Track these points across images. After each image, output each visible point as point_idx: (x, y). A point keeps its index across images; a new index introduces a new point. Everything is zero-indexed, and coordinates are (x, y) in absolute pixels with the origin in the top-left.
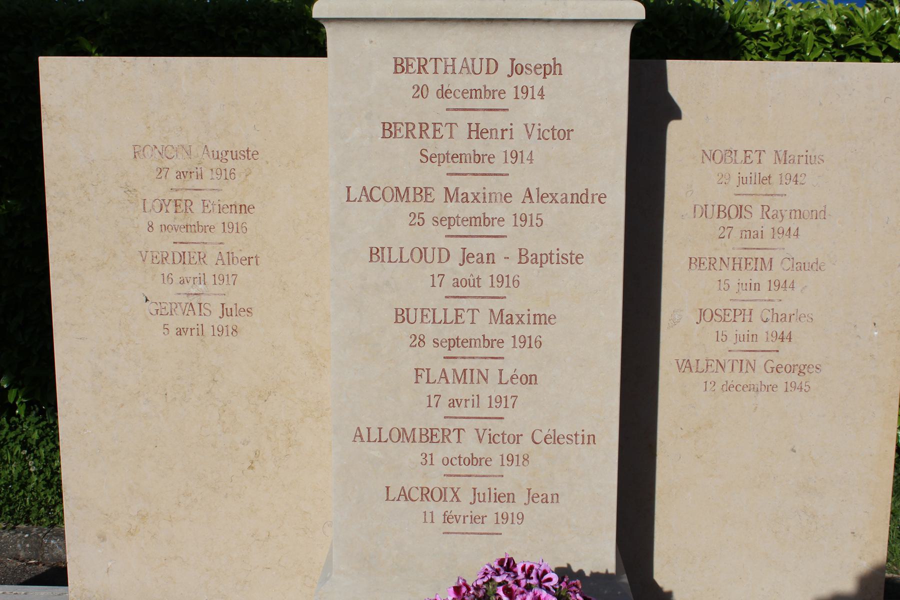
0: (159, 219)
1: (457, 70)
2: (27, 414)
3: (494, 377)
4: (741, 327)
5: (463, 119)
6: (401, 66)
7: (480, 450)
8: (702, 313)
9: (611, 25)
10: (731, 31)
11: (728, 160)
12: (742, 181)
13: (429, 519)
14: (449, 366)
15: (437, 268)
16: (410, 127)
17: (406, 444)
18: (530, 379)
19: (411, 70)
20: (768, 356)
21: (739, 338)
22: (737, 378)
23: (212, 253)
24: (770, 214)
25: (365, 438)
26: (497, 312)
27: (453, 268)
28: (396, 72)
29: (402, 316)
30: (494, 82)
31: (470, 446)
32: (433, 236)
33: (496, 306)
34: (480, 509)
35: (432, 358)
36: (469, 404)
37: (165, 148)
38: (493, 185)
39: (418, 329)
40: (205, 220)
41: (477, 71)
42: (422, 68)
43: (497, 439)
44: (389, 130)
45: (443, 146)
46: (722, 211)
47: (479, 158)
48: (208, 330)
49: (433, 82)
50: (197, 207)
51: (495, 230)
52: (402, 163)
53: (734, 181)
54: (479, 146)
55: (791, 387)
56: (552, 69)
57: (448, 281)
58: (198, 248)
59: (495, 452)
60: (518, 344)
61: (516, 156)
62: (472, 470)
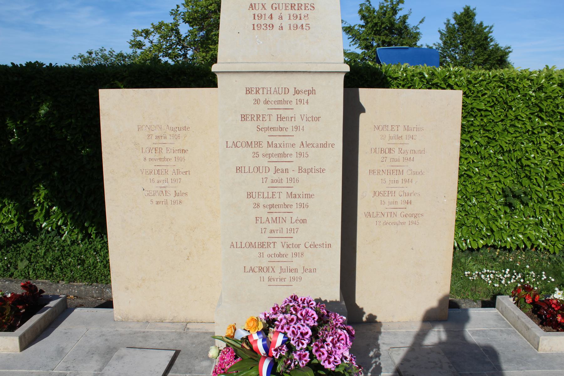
0: (148, 156)
1: (272, 93)
2: (96, 237)
3: (288, 220)
4: (391, 199)
5: (274, 113)
6: (249, 91)
7: (283, 251)
8: (375, 193)
9: (336, 74)
10: (385, 77)
11: (385, 129)
12: (391, 138)
13: (262, 280)
15: (264, 175)
16: (253, 116)
17: (252, 249)
18: (304, 221)
19: (253, 93)
20: (402, 210)
21: (390, 203)
22: (389, 219)
24: (402, 151)
25: (235, 246)
26: (289, 193)
27: (271, 175)
28: (247, 94)
29: (250, 195)
30: (287, 97)
31: (279, 249)
32: (263, 162)
34: (283, 275)
35: (263, 213)
36: (279, 231)
37: (151, 126)
38: (287, 140)
39: (257, 201)
40: (168, 156)
41: (280, 93)
42: (257, 92)
43: (291, 246)
44: (244, 118)
45: (266, 124)
46: (383, 151)
47: (281, 129)
48: (169, 202)
50: (164, 151)
51: (288, 159)
52: (249, 131)
53: (387, 138)
54: (282, 124)
56: (311, 92)
57: (269, 180)
58: (165, 168)
59: (290, 251)
60: (298, 206)
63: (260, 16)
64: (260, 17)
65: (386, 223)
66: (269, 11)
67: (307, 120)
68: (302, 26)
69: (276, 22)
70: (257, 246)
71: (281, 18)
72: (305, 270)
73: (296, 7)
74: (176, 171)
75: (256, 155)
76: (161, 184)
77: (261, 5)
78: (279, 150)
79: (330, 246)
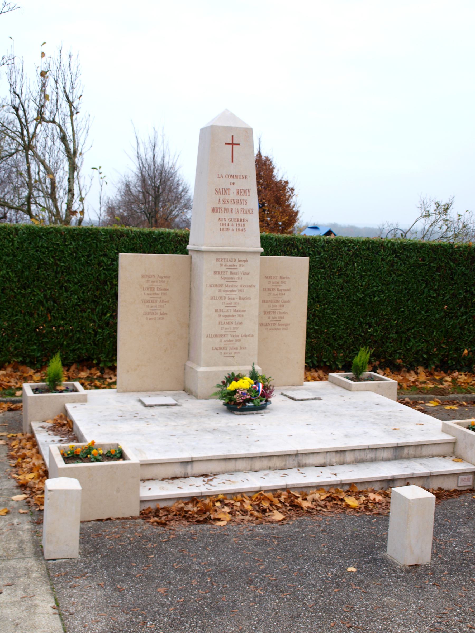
0: (147, 292)
4: (273, 315)
5: (229, 271)
6: (218, 260)
7: (231, 339)
12: (273, 283)
14: (226, 321)
15: (224, 301)
18: (241, 323)
21: (273, 318)
22: (273, 327)
23: (159, 300)
27: (227, 301)
30: (235, 263)
31: (229, 338)
32: (223, 294)
33: (235, 308)
34: (231, 351)
35: (222, 319)
38: (234, 284)
40: (158, 292)
44: (215, 273)
45: (225, 276)
46: (269, 290)
50: (156, 289)
51: (235, 293)
52: (217, 280)
54: (232, 276)
55: (284, 329)
56: (246, 261)
59: (234, 339)
61: (239, 278)
64: (224, 224)
65: (270, 329)
66: (227, 222)
69: (230, 227)
71: (233, 225)
78: (231, 289)
79: (252, 336)
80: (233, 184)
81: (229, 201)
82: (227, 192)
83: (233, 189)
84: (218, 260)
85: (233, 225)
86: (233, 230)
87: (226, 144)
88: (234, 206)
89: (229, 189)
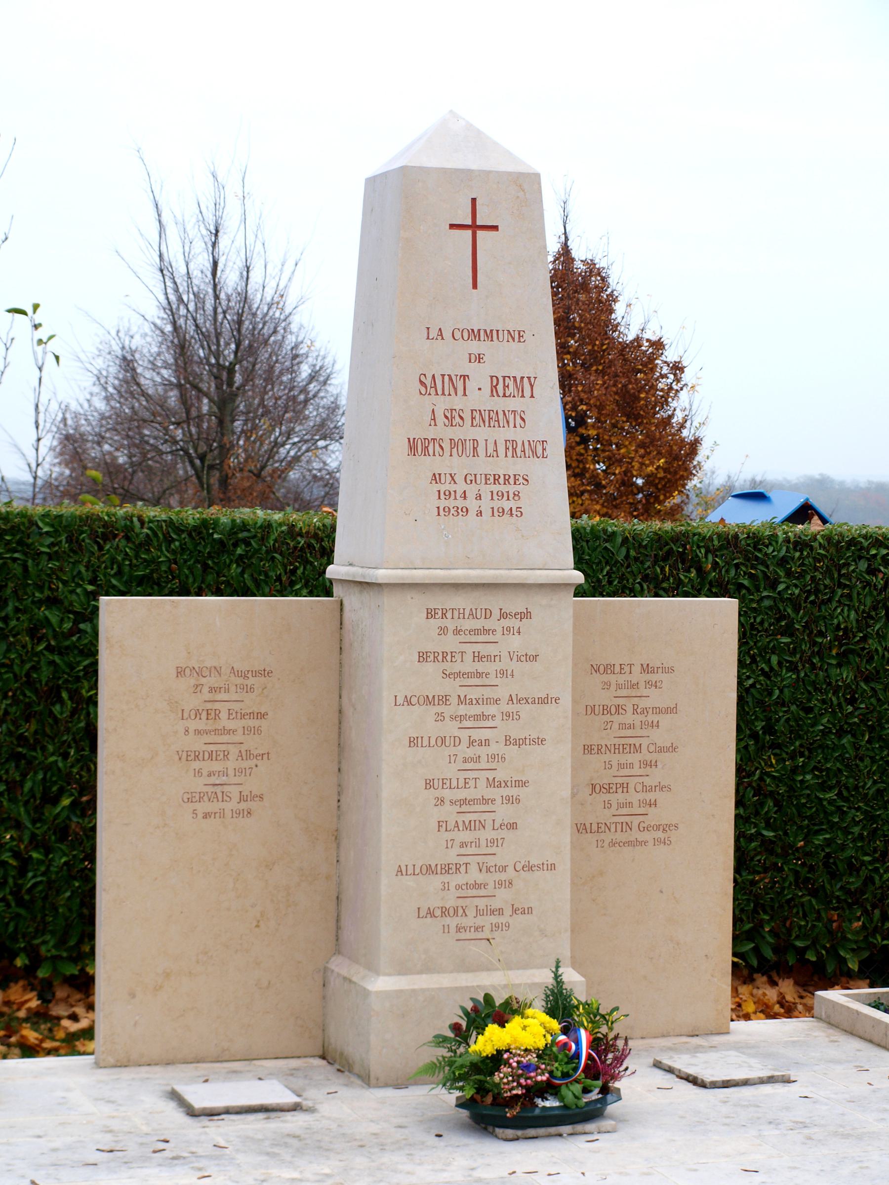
0: (193, 725)
1: (466, 617)
3: (489, 825)
4: (621, 797)
5: (469, 649)
6: (431, 614)
7: (480, 878)
8: (594, 787)
11: (609, 672)
12: (619, 687)
13: (446, 931)
14: (460, 819)
15: (453, 750)
16: (436, 654)
17: (432, 876)
18: (513, 826)
20: (641, 818)
21: (620, 806)
22: (620, 837)
23: (234, 751)
24: (639, 711)
25: (404, 873)
26: (491, 779)
27: (463, 750)
29: (429, 784)
30: (488, 624)
31: (474, 875)
32: (451, 728)
33: (490, 775)
34: (480, 921)
35: (449, 813)
36: (473, 844)
37: (201, 669)
38: (488, 693)
39: (440, 793)
40: (231, 725)
41: (479, 617)
43: (492, 869)
44: (423, 657)
45: (458, 667)
46: (606, 710)
47: (479, 675)
48: (228, 814)
49: (450, 624)
50: (224, 715)
51: (490, 723)
52: (431, 679)
53: (613, 687)
54: (481, 667)
55: (658, 842)
56: (526, 615)
57: (460, 759)
58: (223, 747)
59: (490, 879)
60: (505, 801)
61: (503, 673)
62: (474, 892)
63: (447, 493)
65: (613, 844)
66: (461, 487)
67: (519, 659)
68: (511, 509)
69: (472, 504)
70: (439, 871)
71: (479, 497)
72: (515, 911)
73: (501, 480)
74: (244, 754)
75: (440, 718)
76: (214, 780)
77: (448, 476)
78: (476, 710)
79: (553, 867)
80: (479, 358)
81: (467, 416)
82: (460, 385)
83: (479, 377)
84: (431, 614)
85: (479, 497)
86: (480, 514)
87: (452, 226)
88: (482, 433)
89: (465, 377)
